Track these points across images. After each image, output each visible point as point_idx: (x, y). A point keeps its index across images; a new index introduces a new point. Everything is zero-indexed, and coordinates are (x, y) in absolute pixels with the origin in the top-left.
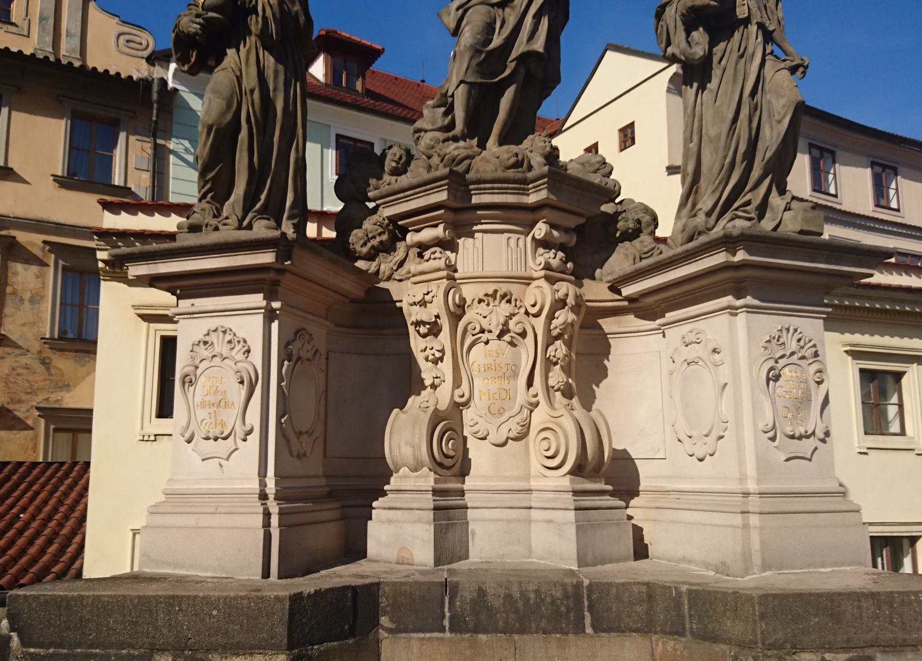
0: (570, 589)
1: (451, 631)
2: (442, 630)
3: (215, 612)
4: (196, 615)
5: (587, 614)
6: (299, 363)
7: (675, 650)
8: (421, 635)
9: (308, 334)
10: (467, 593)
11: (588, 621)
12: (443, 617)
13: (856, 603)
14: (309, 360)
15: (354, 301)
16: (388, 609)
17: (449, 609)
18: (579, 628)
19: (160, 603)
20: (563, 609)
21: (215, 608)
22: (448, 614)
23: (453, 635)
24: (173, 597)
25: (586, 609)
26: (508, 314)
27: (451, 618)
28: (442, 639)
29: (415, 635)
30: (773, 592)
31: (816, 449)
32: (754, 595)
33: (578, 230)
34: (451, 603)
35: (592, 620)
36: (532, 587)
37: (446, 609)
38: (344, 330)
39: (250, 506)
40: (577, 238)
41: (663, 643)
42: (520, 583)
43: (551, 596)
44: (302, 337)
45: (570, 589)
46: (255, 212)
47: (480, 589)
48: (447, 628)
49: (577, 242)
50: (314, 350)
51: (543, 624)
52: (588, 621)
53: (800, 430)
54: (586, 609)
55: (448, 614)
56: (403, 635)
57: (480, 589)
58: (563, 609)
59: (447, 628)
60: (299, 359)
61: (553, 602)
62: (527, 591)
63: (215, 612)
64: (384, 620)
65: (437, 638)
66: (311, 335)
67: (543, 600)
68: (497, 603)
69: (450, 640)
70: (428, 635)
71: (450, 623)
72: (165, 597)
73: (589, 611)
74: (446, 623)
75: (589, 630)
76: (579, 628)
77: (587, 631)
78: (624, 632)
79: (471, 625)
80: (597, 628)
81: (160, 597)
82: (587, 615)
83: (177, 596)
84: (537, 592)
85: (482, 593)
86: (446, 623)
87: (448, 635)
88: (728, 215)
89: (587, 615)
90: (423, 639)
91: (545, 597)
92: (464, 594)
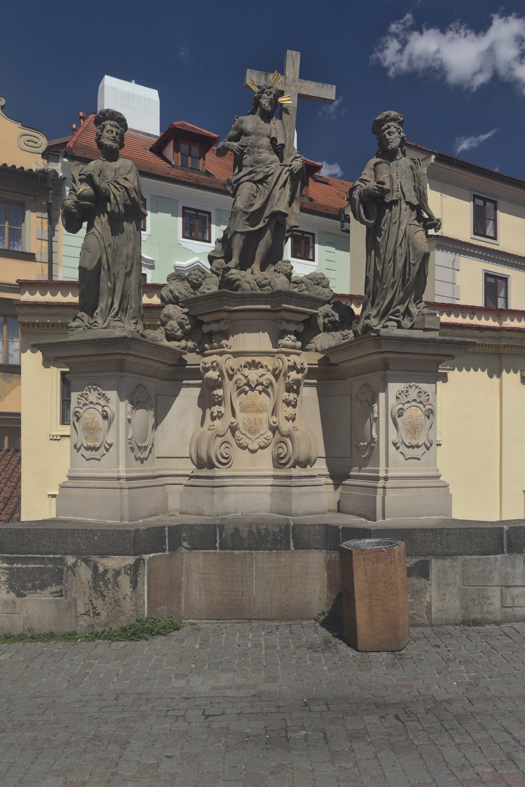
0: (283, 528)
1: (220, 549)
2: (215, 548)
3: (96, 538)
4: (86, 539)
5: (291, 540)
6: (138, 404)
7: (335, 557)
8: (204, 551)
9: (143, 387)
10: (229, 530)
11: (292, 544)
12: (216, 542)
13: (423, 534)
14: (144, 403)
15: (170, 365)
16: (187, 538)
17: (219, 538)
18: (287, 548)
19: (68, 533)
20: (279, 538)
21: (96, 536)
22: (218, 541)
23: (221, 551)
24: (74, 530)
25: (291, 538)
26: (261, 375)
27: (220, 543)
28: (215, 553)
29: (201, 551)
30: (381, 528)
31: (424, 453)
32: (371, 530)
33: (304, 322)
34: (221, 536)
35: (294, 544)
36: (263, 527)
37: (218, 538)
38: (167, 382)
40: (304, 326)
41: (331, 555)
42: (257, 525)
43: (273, 531)
44: (140, 389)
45: (283, 528)
46: (111, 317)
47: (236, 528)
48: (218, 548)
49: (304, 329)
50: (147, 396)
51: (269, 545)
52: (292, 544)
53: (414, 443)
54: (291, 538)
55: (218, 541)
56: (195, 551)
57: (236, 528)
58: (279, 538)
59: (218, 548)
60: (138, 402)
61: (274, 534)
62: (260, 529)
63: (96, 538)
64: (185, 544)
65: (213, 553)
66: (145, 388)
67: (269, 533)
68: (245, 535)
69: (220, 553)
70: (208, 551)
71: (219, 545)
72: (71, 530)
73: (292, 539)
74: (217, 545)
75: (292, 548)
76: (287, 548)
77: (291, 549)
78: (310, 549)
79: (231, 546)
80: (296, 547)
81: (68, 530)
82: (291, 540)
83: (77, 529)
84: (266, 529)
85: (236, 530)
86: (217, 545)
87: (218, 551)
88: (386, 318)
90: (205, 553)
91: (270, 532)
92: (227, 530)
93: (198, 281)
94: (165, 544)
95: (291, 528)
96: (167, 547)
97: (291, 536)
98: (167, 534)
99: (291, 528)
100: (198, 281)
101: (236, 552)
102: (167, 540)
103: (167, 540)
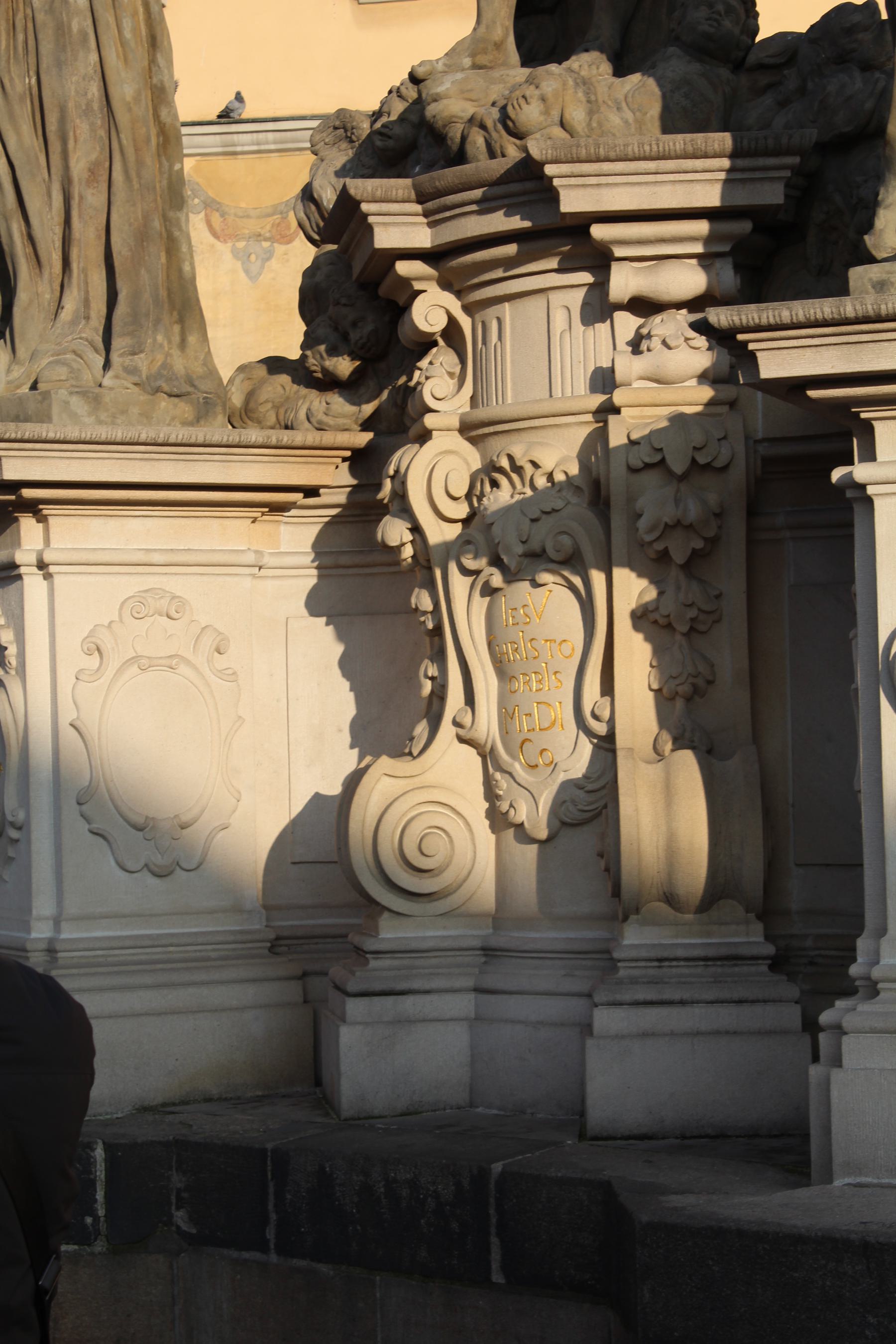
8: (234, 1254)
11: (496, 1256)
22: (273, 1217)
25: (493, 1230)
37: (271, 1207)
39: (109, 973)
48: (272, 1246)
54: (493, 1230)
55: (273, 1217)
59: (272, 1246)
70: (246, 1255)
74: (270, 1234)
82: (494, 1240)
86: (270, 1234)
87: (274, 1258)
89: (494, 1240)
93: (390, 137)
94: (93, 1213)
95: (492, 1186)
96: (103, 1227)
97: (494, 1220)
98: (100, 1172)
99: (492, 1186)
100: (390, 137)
101: (324, 1268)
102: (100, 1195)
103: (100, 1195)
